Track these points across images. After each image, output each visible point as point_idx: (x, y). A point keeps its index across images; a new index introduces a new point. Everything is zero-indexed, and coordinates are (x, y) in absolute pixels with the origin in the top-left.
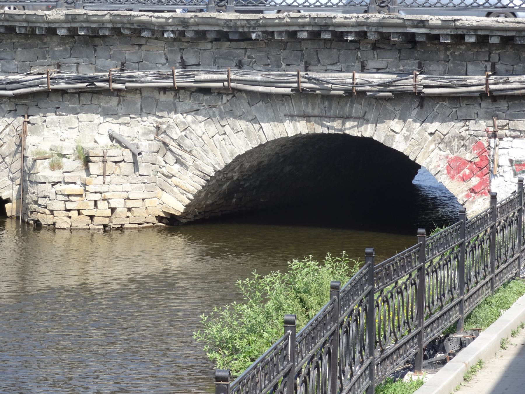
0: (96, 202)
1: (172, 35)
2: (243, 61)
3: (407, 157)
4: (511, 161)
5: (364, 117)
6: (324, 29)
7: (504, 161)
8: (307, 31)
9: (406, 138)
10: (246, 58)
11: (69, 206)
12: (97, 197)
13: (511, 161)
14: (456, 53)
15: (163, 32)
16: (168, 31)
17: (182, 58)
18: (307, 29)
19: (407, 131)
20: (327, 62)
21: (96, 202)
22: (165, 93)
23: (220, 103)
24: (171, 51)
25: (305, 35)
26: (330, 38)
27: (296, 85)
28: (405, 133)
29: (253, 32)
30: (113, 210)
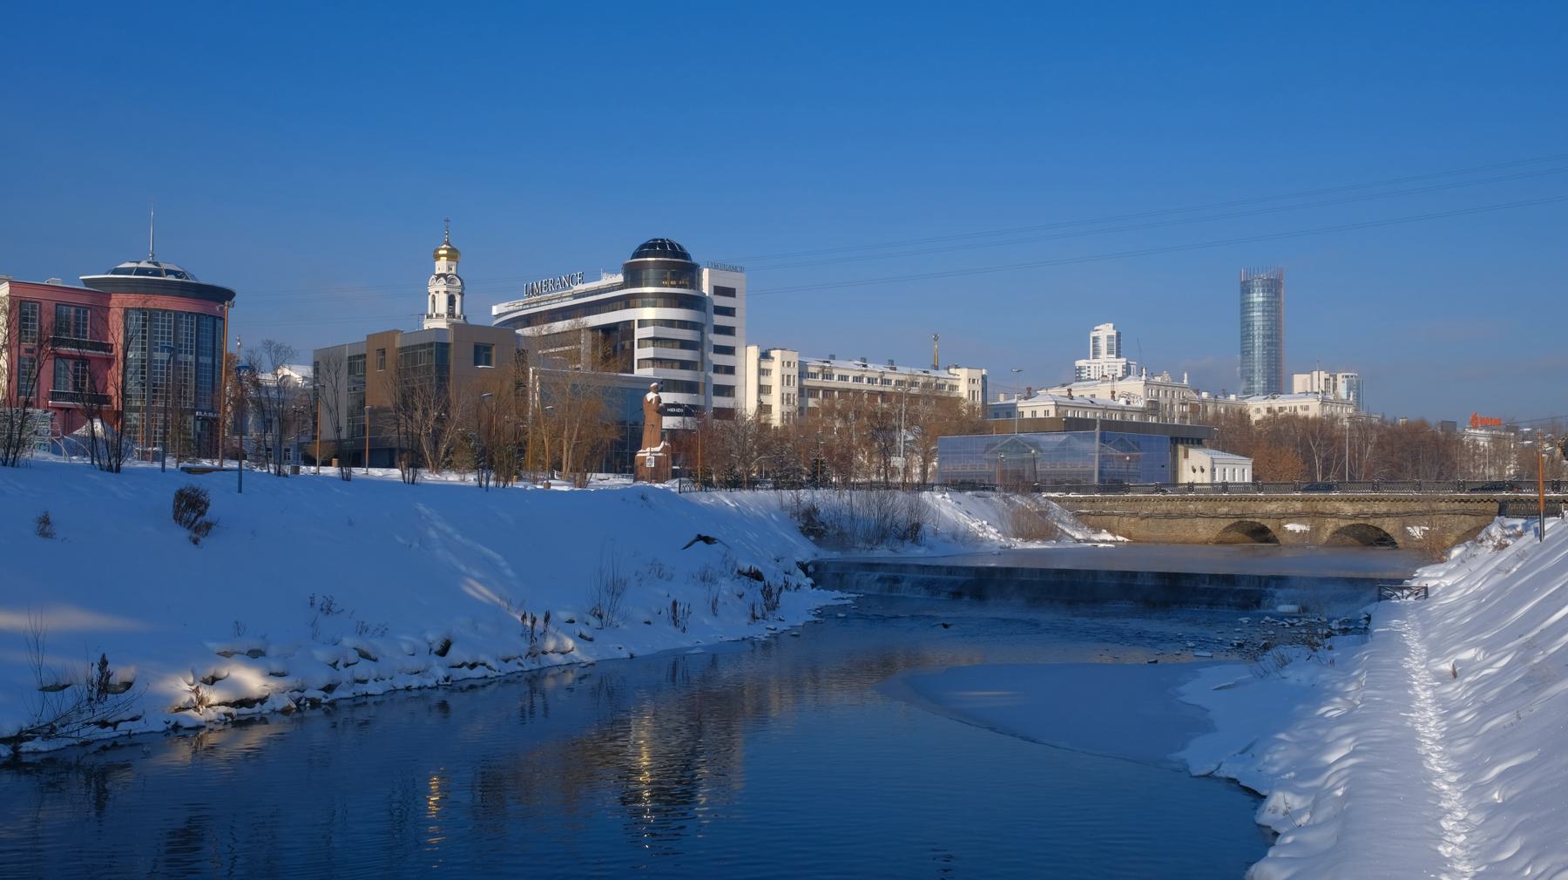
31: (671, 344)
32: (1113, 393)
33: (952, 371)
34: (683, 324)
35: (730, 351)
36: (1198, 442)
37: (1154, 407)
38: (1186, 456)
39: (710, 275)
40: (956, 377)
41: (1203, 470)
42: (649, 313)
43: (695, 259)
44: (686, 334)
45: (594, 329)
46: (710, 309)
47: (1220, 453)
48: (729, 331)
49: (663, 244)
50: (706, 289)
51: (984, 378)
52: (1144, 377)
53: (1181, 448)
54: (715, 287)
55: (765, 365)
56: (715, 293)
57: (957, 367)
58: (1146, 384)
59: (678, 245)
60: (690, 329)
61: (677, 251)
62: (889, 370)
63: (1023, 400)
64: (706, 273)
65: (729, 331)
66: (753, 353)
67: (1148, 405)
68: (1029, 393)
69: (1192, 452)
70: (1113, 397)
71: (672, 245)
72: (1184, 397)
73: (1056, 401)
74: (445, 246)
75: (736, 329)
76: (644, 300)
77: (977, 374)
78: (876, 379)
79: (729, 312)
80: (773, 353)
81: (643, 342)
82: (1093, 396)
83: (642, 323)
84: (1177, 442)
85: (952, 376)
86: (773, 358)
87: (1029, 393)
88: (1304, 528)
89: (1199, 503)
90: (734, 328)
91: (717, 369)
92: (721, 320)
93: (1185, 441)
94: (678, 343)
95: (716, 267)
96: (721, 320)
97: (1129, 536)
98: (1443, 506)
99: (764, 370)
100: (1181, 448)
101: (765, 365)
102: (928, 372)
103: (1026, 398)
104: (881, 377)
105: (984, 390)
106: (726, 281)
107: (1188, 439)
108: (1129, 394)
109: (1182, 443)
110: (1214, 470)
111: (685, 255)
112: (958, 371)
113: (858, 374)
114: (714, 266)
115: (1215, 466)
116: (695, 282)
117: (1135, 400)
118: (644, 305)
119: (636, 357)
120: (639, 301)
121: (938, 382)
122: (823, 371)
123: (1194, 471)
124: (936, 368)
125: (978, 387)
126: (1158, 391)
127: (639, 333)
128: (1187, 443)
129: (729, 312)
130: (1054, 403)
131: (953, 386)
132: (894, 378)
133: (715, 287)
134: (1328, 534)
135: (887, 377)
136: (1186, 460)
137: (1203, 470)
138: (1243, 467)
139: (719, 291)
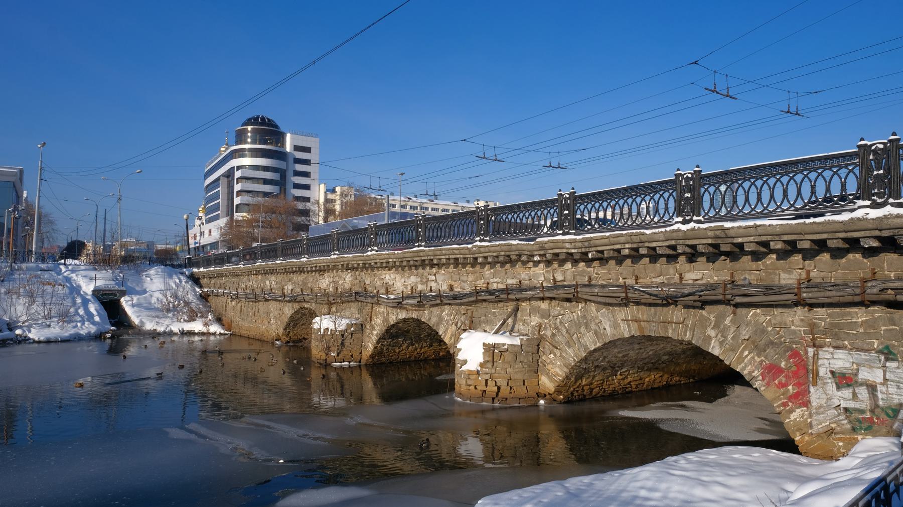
0: (486, 380)
1: (539, 259)
2: (592, 277)
3: (722, 361)
4: (832, 372)
5: (683, 322)
6: (641, 245)
7: (822, 371)
8: (628, 248)
9: (721, 343)
10: (595, 275)
11: (469, 382)
12: (487, 377)
13: (832, 372)
14: (768, 263)
15: (533, 256)
16: (536, 255)
17: (553, 276)
18: (627, 246)
19: (722, 336)
20: (652, 275)
21: (486, 380)
22: (543, 302)
23: (576, 310)
24: (547, 271)
25: (626, 252)
26: (646, 253)
27: (624, 295)
28: (720, 339)
29: (590, 252)
30: (499, 388)
31: (257, 182)
34: (266, 169)
35: (307, 187)
39: (292, 139)
42: (247, 161)
43: (282, 129)
44: (268, 175)
45: (223, 175)
46: (291, 160)
48: (306, 174)
49: (256, 119)
50: (288, 148)
54: (294, 146)
55: (330, 196)
56: (294, 150)
59: (268, 119)
60: (271, 172)
61: (270, 123)
62: (428, 202)
64: (288, 137)
65: (306, 174)
66: (322, 187)
71: (263, 119)
74: (225, 146)
75: (311, 173)
76: (240, 153)
78: (417, 207)
79: (307, 162)
80: (338, 189)
81: (240, 179)
83: (239, 168)
86: (337, 192)
88: (343, 324)
89: (273, 278)
90: (310, 172)
91: (297, 198)
92: (300, 167)
94: (262, 181)
95: (295, 134)
96: (300, 167)
97: (229, 328)
98: (539, 275)
99: (329, 199)
101: (330, 196)
102: (457, 203)
104: (420, 205)
106: (303, 142)
111: (276, 126)
113: (403, 203)
114: (294, 133)
116: (283, 144)
118: (240, 157)
119: (236, 190)
120: (237, 154)
122: (376, 201)
124: (468, 202)
127: (238, 174)
129: (307, 162)
132: (430, 206)
133: (294, 146)
134: (374, 338)
135: (425, 205)
139: (297, 148)
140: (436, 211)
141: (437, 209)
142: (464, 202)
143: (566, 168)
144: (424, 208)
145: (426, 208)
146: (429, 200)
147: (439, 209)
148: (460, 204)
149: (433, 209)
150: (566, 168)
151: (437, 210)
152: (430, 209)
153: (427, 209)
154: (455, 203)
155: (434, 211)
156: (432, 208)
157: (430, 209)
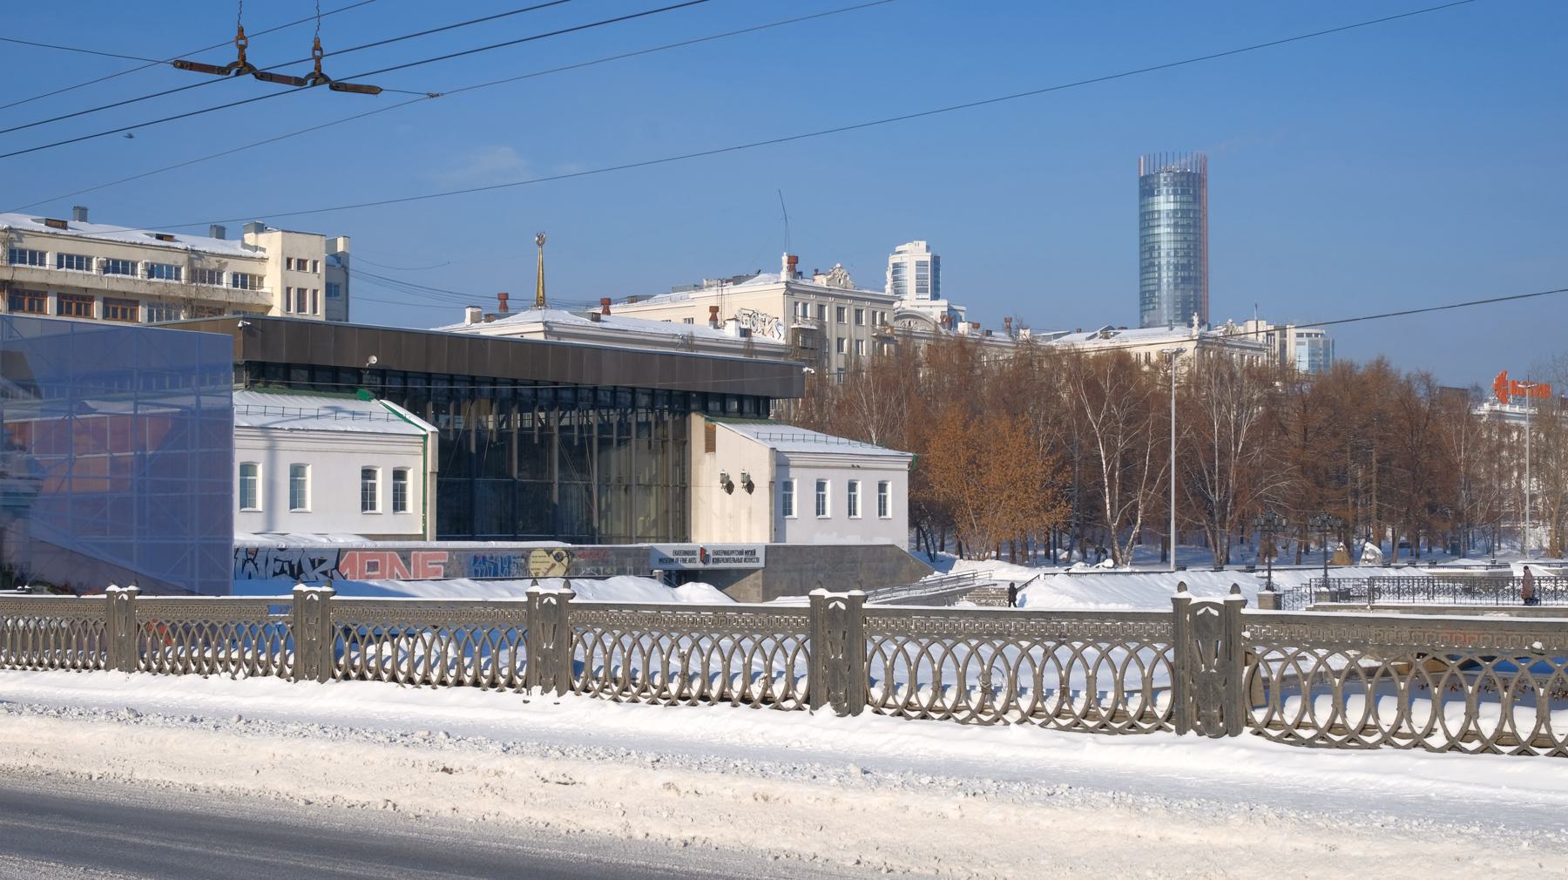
32: (714, 310)
33: (250, 238)
36: (754, 408)
37: (810, 343)
38: (710, 446)
40: (259, 254)
41: (750, 487)
47: (810, 434)
51: (338, 265)
52: (784, 275)
53: (698, 423)
57: (260, 229)
58: (790, 290)
62: (42, 227)
63: (483, 323)
67: (795, 338)
68: (504, 307)
69: (724, 431)
70: (714, 319)
72: (883, 323)
73: (545, 324)
77: (312, 248)
82: (690, 321)
84: (686, 413)
85: (248, 253)
87: (504, 307)
93: (714, 406)
100: (698, 423)
102: (170, 238)
103: (489, 318)
105: (332, 290)
107: (723, 398)
108: (753, 315)
109: (704, 410)
110: (788, 486)
112: (262, 239)
115: (793, 473)
117: (767, 327)
121: (198, 264)
123: (729, 488)
124: (220, 233)
125: (314, 281)
126: (821, 308)
128: (576, 390)
130: (541, 327)
131: (244, 276)
135: (29, 244)
136: (708, 456)
137: (750, 487)
138: (821, 474)
140: (80, 267)
141: (80, 258)
142: (203, 235)
143: (373, 90)
144: (23, 252)
145: (33, 253)
146: (49, 223)
147: (89, 260)
148: (185, 241)
149: (64, 260)
150: (373, 90)
151: (82, 262)
152: (50, 259)
153: (36, 257)
154: (160, 237)
155: (70, 266)
156: (60, 257)
157: (50, 259)
